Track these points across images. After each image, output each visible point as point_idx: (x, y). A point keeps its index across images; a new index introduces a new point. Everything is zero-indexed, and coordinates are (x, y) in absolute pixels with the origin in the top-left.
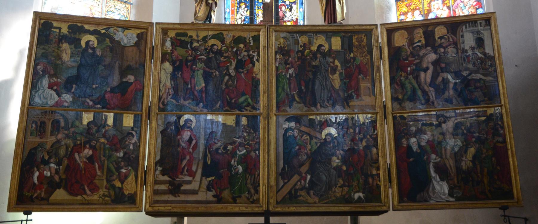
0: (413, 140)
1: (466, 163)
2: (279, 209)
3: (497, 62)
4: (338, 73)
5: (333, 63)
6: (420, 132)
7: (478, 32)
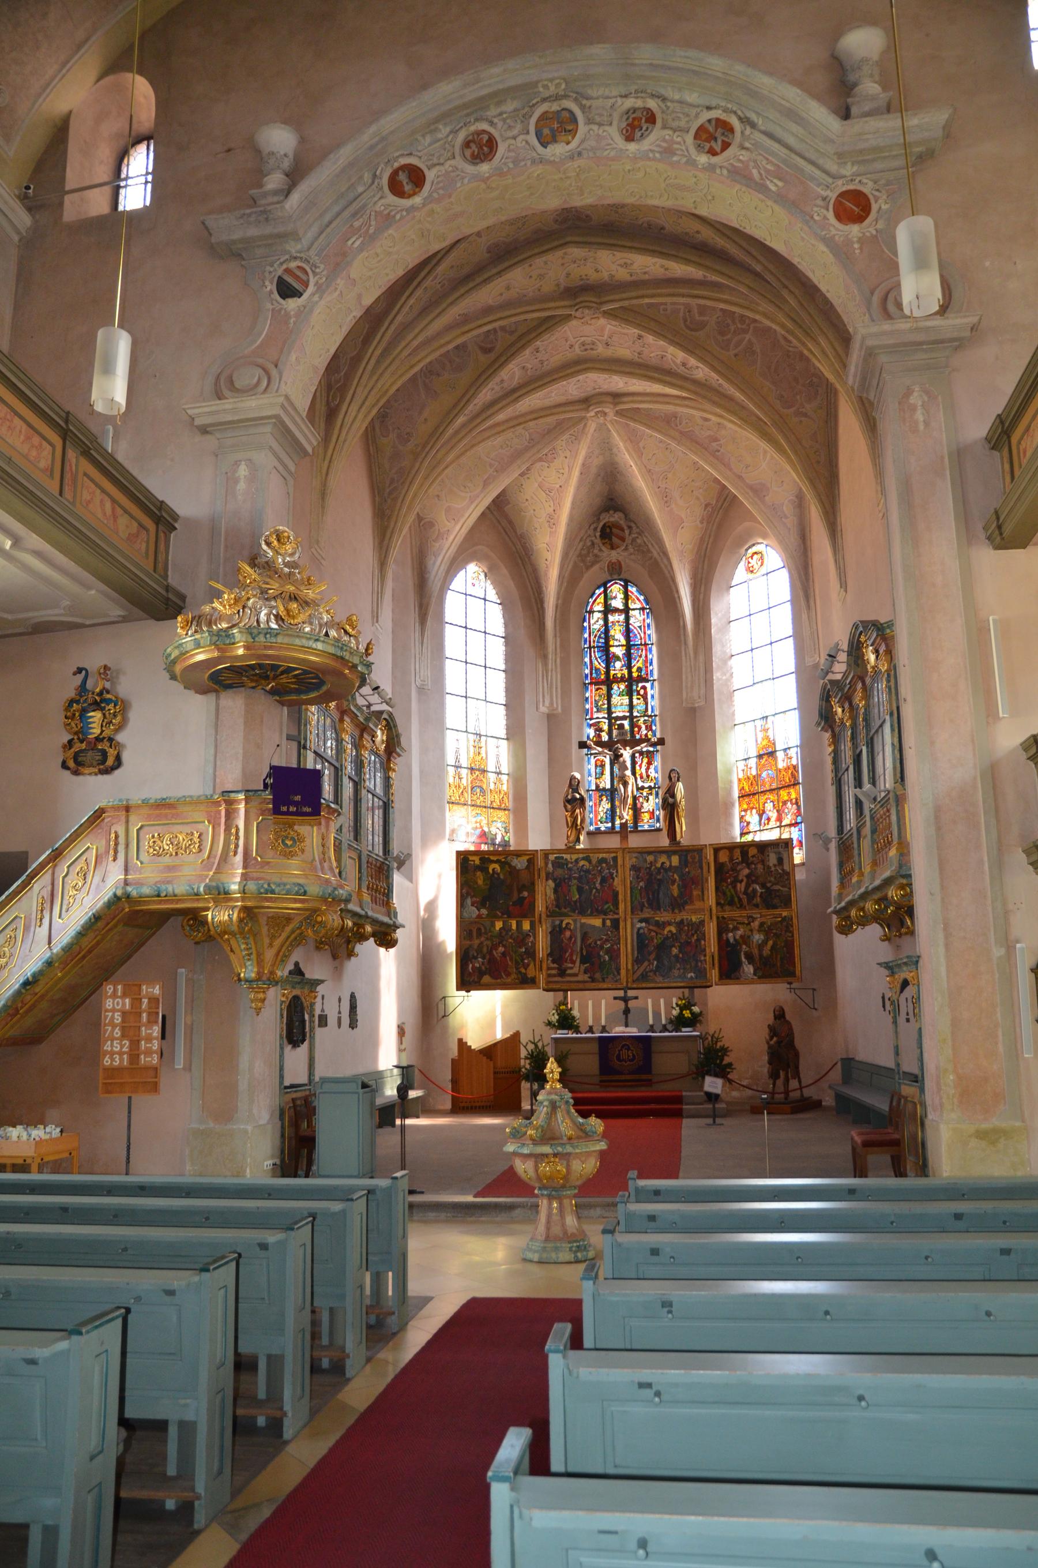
0: (730, 935)
1: (766, 952)
2: (635, 986)
6: (736, 929)
7: (779, 853)
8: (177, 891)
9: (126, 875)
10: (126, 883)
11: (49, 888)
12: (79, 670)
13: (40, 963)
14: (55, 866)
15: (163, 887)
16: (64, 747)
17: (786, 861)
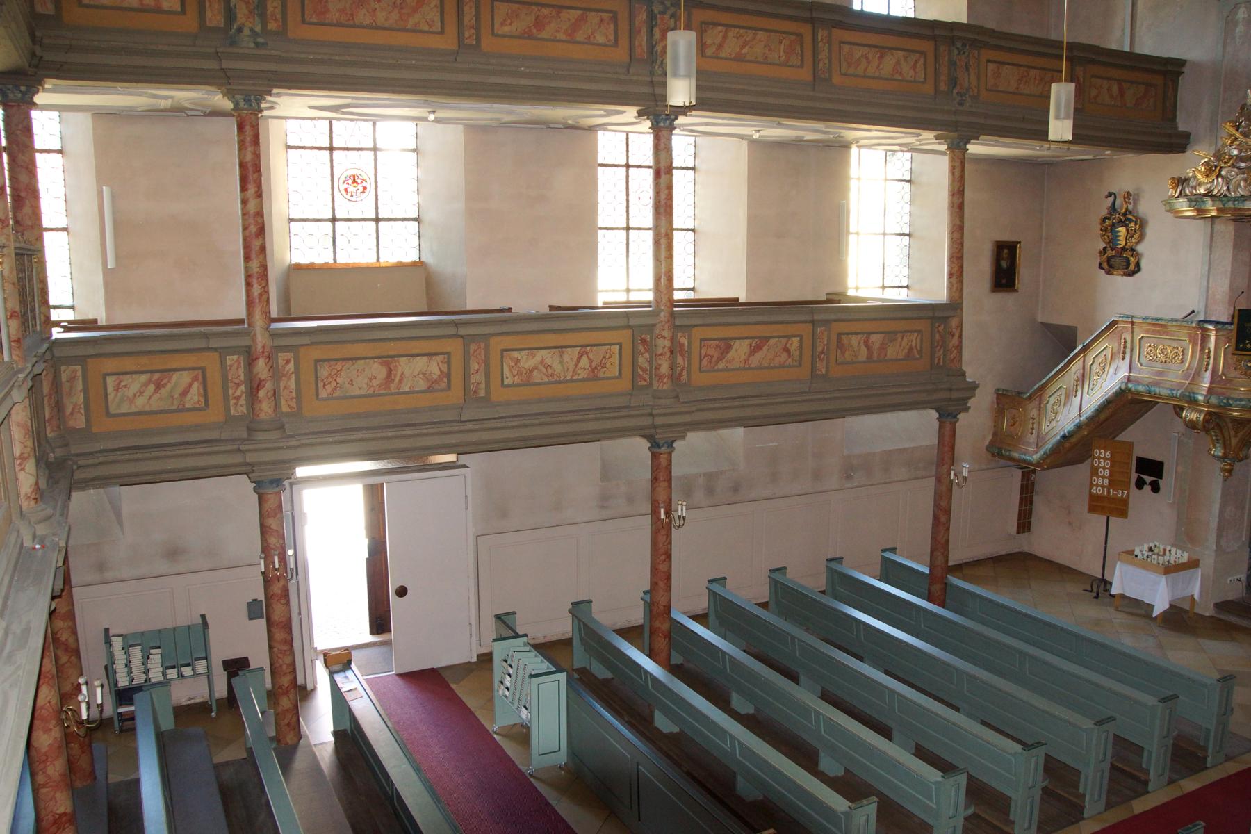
8: (1161, 393)
9: (1130, 372)
10: (1129, 379)
11: (1082, 371)
12: (1110, 194)
13: (1073, 425)
14: (1084, 356)
15: (1153, 389)
16: (1100, 252)
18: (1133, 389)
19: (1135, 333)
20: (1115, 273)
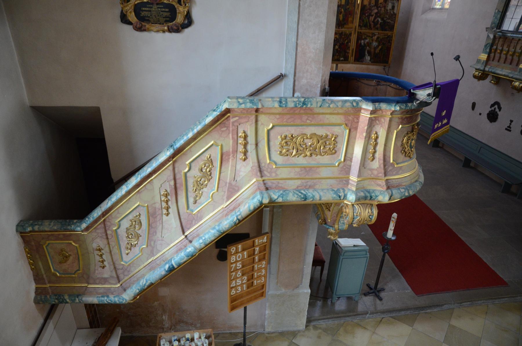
0: (363, 41)
1: (377, 51)
3: (397, 16)
4: (342, 14)
5: (341, 10)
6: (366, 39)
7: (394, 3)
9: (262, 177)
11: (172, 183)
17: (396, 8)
18: (280, 200)
19: (259, 123)
20: (152, 28)
